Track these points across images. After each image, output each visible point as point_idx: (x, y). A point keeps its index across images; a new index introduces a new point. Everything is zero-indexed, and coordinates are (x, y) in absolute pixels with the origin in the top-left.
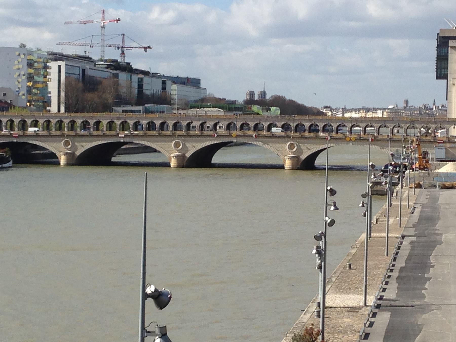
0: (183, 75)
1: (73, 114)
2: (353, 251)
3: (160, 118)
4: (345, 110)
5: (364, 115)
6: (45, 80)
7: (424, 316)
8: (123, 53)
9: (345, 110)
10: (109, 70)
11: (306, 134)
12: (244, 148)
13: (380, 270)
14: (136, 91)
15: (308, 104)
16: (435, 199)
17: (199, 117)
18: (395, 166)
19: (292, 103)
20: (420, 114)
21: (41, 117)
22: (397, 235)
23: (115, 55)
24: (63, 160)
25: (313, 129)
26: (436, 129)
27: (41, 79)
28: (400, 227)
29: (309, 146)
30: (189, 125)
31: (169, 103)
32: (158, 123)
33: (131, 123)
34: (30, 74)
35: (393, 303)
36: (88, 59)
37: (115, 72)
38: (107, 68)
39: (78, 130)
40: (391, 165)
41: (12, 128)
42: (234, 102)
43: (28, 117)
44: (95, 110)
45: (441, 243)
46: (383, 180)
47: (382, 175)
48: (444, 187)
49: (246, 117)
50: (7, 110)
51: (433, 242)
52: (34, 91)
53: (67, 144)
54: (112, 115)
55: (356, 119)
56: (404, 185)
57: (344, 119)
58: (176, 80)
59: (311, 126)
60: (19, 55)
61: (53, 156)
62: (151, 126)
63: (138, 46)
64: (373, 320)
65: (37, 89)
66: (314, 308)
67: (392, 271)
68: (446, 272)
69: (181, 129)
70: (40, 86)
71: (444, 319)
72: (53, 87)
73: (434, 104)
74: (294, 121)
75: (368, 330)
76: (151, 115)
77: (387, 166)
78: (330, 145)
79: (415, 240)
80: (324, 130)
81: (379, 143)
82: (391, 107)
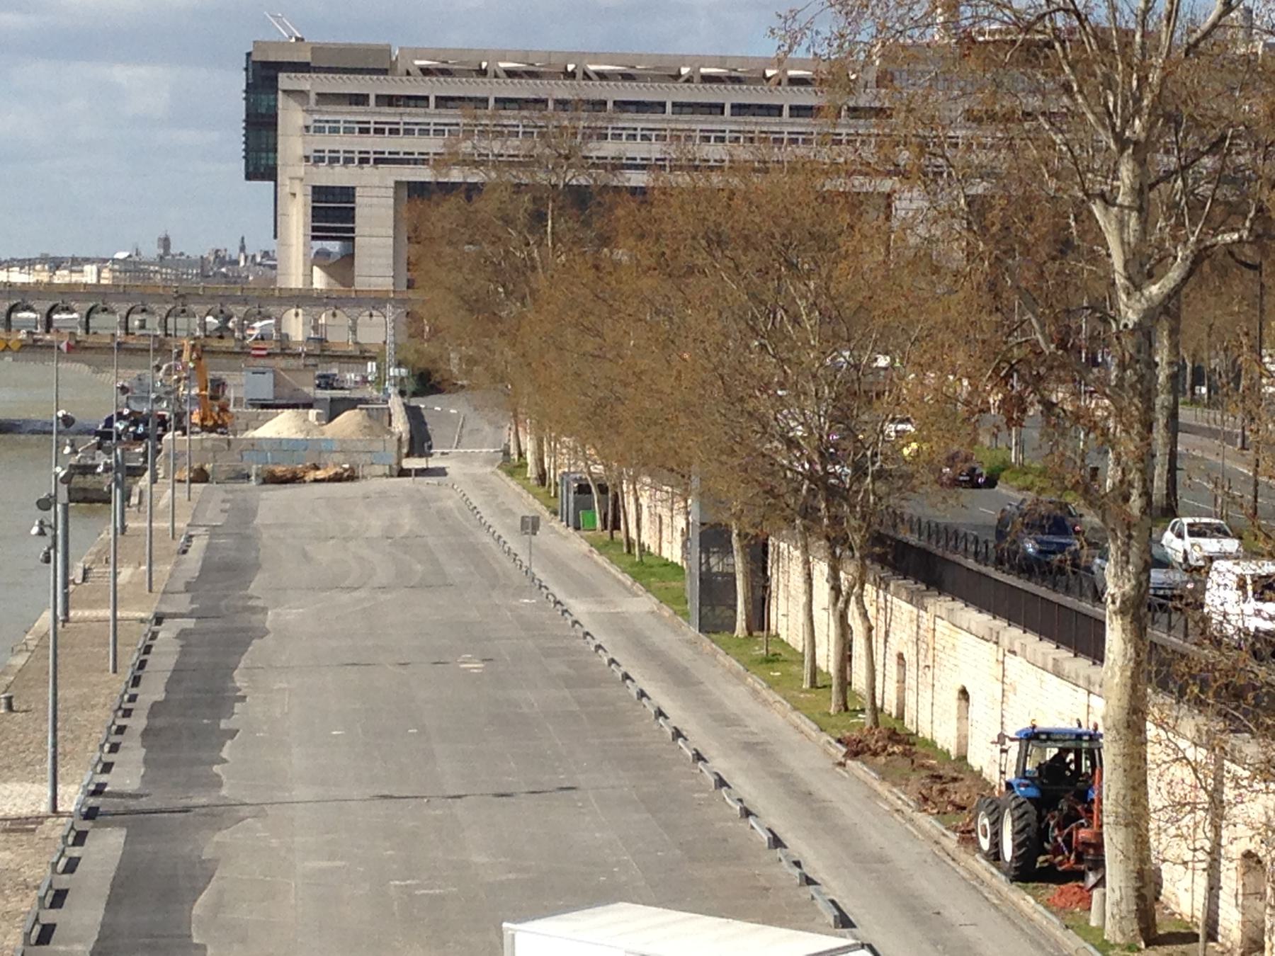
2: (19, 661)
13: (96, 712)
16: (245, 513)
22: (143, 615)
28: (150, 591)
45: (264, 633)
48: (272, 479)
51: (243, 630)
67: (127, 713)
73: (242, 249)
79: (192, 626)
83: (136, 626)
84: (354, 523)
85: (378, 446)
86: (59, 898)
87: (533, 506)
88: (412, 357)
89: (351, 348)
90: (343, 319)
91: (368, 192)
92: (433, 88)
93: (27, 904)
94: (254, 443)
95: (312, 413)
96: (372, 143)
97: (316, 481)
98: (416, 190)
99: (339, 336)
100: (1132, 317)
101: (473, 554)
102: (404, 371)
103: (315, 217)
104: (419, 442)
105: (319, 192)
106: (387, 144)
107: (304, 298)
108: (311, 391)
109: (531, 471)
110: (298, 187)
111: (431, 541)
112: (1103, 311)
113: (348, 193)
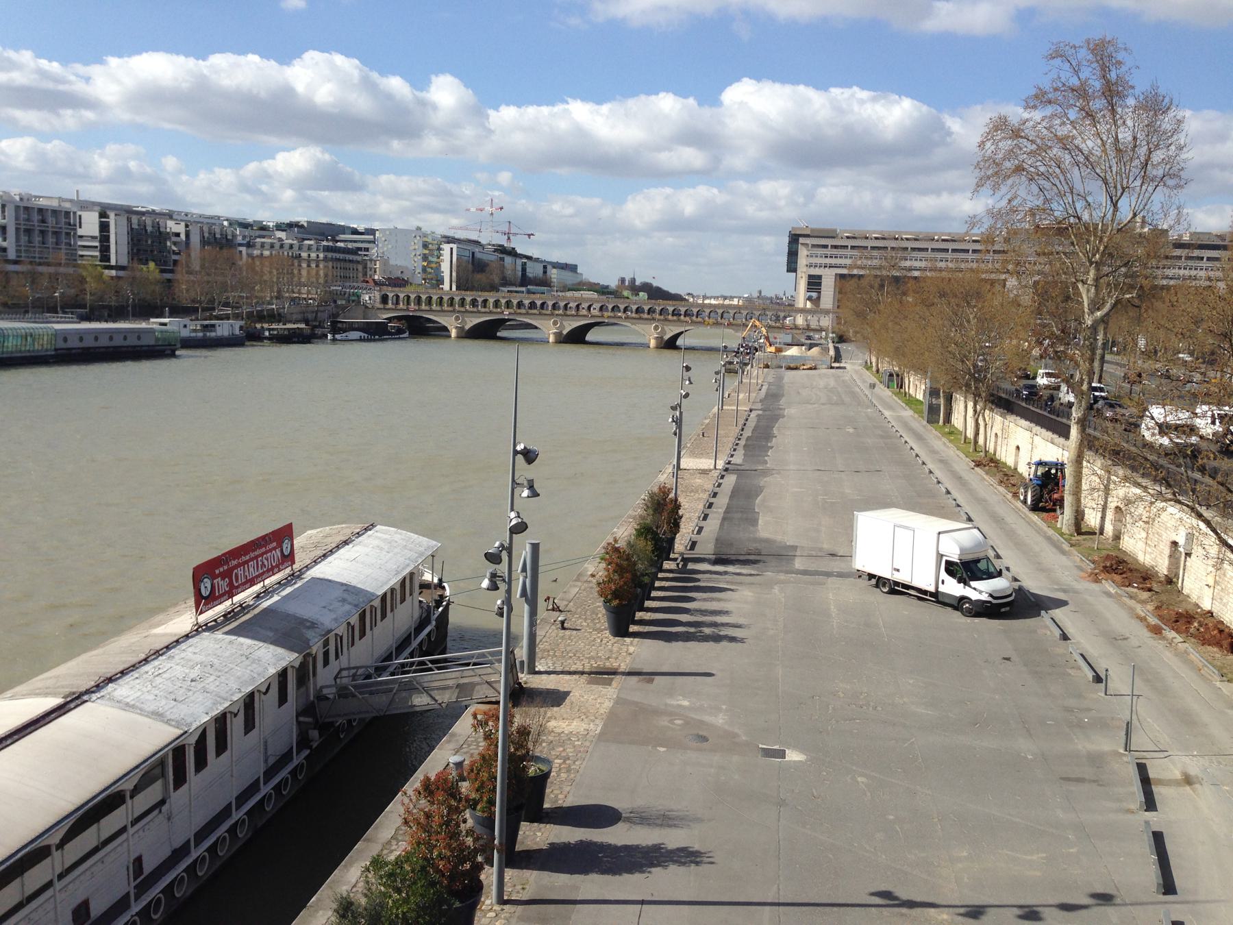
0: (562, 261)
1: (463, 292)
2: (707, 421)
4: (705, 297)
5: (721, 302)
6: (438, 260)
7: (765, 479)
8: (509, 238)
9: (705, 297)
10: (496, 254)
11: (670, 317)
12: (615, 327)
14: (520, 273)
15: (673, 291)
16: (780, 378)
18: (747, 347)
19: (659, 290)
21: (434, 294)
24: (454, 333)
25: (676, 313)
26: (785, 318)
27: (435, 259)
29: (672, 328)
30: (566, 305)
32: (539, 303)
33: (515, 302)
34: (425, 254)
35: (739, 467)
36: (477, 243)
37: (502, 256)
38: (494, 252)
39: (457, 306)
40: (742, 347)
41: (408, 303)
42: (607, 287)
44: (483, 290)
45: (784, 416)
46: (736, 360)
47: (735, 356)
48: (789, 368)
49: (617, 300)
53: (457, 318)
54: (497, 294)
55: (715, 306)
57: (704, 305)
58: (557, 265)
59: (674, 310)
61: (445, 329)
62: (533, 305)
63: (523, 233)
64: (721, 481)
65: (432, 268)
66: (670, 470)
67: (739, 439)
70: (434, 265)
71: (783, 482)
72: (445, 267)
74: (659, 305)
75: (717, 490)
77: (739, 349)
78: (690, 328)
80: (686, 315)
81: (733, 327)
82: (746, 296)
83: (744, 413)
84: (815, 383)
85: (824, 359)
87: (874, 380)
88: (837, 330)
89: (818, 328)
90: (816, 318)
92: (850, 243)
94: (784, 356)
95: (804, 347)
96: (828, 261)
98: (842, 276)
100: (1089, 323)
101: (853, 395)
103: (808, 285)
104: (838, 358)
105: (810, 277)
106: (833, 261)
107: (803, 311)
108: (803, 340)
109: (874, 369)
110: (803, 275)
111: (839, 389)
112: (1079, 320)
113: (820, 277)
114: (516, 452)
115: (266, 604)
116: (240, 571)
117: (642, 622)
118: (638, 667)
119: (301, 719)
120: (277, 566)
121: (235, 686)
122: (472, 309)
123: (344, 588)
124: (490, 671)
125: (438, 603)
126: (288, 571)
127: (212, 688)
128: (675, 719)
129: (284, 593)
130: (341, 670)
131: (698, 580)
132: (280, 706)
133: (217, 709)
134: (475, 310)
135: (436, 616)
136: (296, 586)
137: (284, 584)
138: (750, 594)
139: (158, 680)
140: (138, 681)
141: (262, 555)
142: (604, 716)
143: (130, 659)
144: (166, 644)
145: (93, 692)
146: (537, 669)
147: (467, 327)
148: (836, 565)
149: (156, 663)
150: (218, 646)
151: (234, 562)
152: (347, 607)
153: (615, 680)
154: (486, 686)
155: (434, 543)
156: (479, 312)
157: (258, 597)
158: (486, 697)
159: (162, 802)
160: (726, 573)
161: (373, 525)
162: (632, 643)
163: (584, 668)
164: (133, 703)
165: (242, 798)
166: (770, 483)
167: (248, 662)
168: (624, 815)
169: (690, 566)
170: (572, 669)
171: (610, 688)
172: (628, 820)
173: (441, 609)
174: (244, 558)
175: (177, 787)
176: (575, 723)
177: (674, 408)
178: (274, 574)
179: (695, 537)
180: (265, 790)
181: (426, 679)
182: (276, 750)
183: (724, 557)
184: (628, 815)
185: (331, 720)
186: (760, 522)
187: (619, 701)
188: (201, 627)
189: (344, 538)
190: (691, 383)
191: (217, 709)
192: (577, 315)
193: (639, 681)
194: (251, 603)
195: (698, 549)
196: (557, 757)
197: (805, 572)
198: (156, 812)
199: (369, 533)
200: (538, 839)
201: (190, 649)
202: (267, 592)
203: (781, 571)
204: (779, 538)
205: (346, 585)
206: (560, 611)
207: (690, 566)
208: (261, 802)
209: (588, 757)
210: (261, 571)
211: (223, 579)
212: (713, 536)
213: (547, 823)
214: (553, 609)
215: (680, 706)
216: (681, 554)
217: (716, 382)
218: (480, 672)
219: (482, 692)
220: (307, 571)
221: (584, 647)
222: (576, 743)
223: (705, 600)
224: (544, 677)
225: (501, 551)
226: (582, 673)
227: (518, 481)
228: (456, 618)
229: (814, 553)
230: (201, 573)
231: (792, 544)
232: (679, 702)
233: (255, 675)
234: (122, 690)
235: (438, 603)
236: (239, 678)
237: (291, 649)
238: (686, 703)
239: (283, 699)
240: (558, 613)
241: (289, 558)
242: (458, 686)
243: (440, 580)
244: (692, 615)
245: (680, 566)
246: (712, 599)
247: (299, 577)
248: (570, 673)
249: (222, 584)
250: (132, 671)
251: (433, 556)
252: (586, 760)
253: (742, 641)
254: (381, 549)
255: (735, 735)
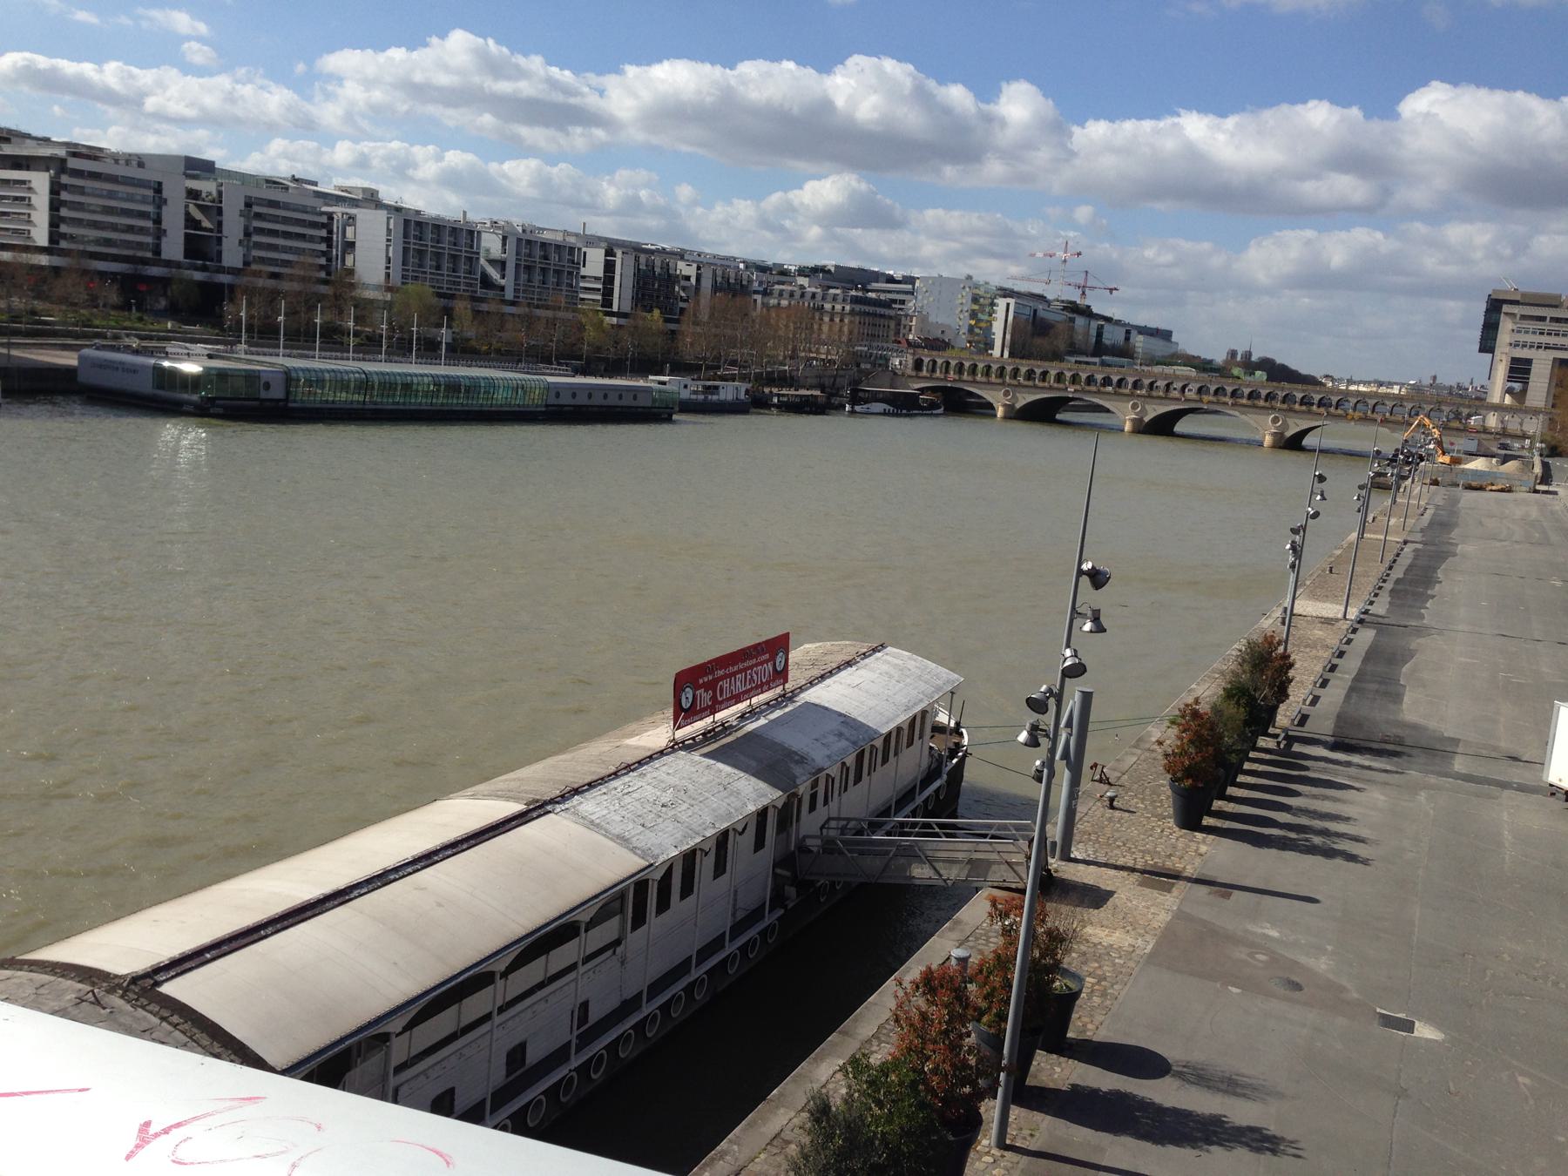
0: (1153, 325)
1: (1018, 361)
2: (1338, 552)
3: (1119, 373)
5: (1374, 389)
6: (989, 319)
7: (1418, 641)
8: (1084, 293)
9: (1350, 382)
11: (1297, 407)
14: (1094, 339)
15: (1304, 371)
16: (1454, 501)
17: (1166, 377)
18: (1410, 454)
20: (1451, 394)
21: (981, 361)
23: (1075, 296)
24: (1000, 412)
25: (1306, 401)
26: (1469, 416)
27: (985, 317)
30: (1152, 384)
31: (1132, 358)
32: (1115, 379)
33: (1084, 376)
34: (973, 311)
35: (1380, 620)
36: (1041, 298)
37: (1071, 315)
38: (1063, 310)
41: (947, 371)
42: (1210, 362)
43: (967, 359)
44: (1043, 358)
45: (1455, 555)
46: (1389, 471)
48: (1469, 487)
49: (1223, 380)
50: (944, 349)
51: (1443, 552)
52: (977, 330)
53: (1007, 393)
54: (1063, 365)
56: (1416, 479)
57: (1348, 393)
58: (1143, 331)
59: (1303, 398)
60: (964, 288)
61: (990, 406)
62: (1107, 381)
63: (1102, 286)
64: (1352, 636)
65: (981, 328)
66: (1278, 613)
67: (1384, 581)
68: (1456, 591)
69: (1141, 388)
70: (983, 325)
72: (998, 328)
73: (1471, 383)
74: (1283, 389)
75: (1345, 648)
76: (1108, 369)
77: (1396, 455)
80: (1320, 404)
81: (1390, 425)
82: (1412, 382)
83: (1394, 544)
84: (1507, 511)
85: (1525, 478)
86: (1341, 654)
88: (1549, 438)
89: (1519, 433)
90: (1517, 419)
91: (1539, 361)
93: (1327, 654)
94: (1463, 470)
95: (1494, 460)
96: (1545, 339)
97: (1491, 490)
99: (1513, 425)
102: (1544, 445)
103: (1510, 372)
104: (1546, 478)
105: (1514, 360)
106: (1552, 340)
108: (1495, 450)
110: (1504, 358)
111: (1545, 524)
113: (1529, 362)
114: (1080, 572)
115: (751, 727)
116: (725, 684)
117: (1220, 815)
118: (1210, 873)
119: (779, 871)
120: (768, 683)
121: (709, 820)
122: (1027, 383)
123: (842, 719)
124: (1011, 848)
125: (953, 753)
126: (779, 690)
127: (684, 817)
128: (1257, 953)
129: (773, 716)
130: (829, 819)
131: (1307, 769)
132: (756, 851)
133: (688, 844)
134: (1030, 383)
135: (948, 768)
136: (787, 710)
137: (773, 706)
138: (1382, 798)
139: (627, 799)
140: (605, 797)
141: (751, 668)
142: (1158, 932)
143: (599, 770)
144: (639, 759)
145: (558, 803)
146: (1072, 856)
147: (1018, 406)
148: (1516, 774)
149: (626, 779)
150: (694, 769)
151: (721, 673)
152: (844, 743)
153: (1177, 886)
154: (1005, 867)
155: (956, 676)
156: (1035, 387)
157: (742, 717)
158: (1004, 881)
159: (617, 943)
160: (1348, 764)
161: (883, 646)
162: (1204, 842)
163: (1135, 864)
164: (598, 821)
165: (705, 953)
166: (1427, 650)
167: (725, 794)
168: (1175, 1068)
169: (1297, 748)
170: (1119, 863)
171: (1169, 895)
172: (1180, 1075)
173: (955, 761)
174: (732, 669)
175: (634, 928)
176: (1117, 934)
177: (1295, 531)
178: (762, 692)
179: (1306, 709)
180: (730, 948)
181: (930, 846)
182: (748, 901)
183: (1347, 741)
184: (1180, 1069)
185: (812, 878)
186: (1406, 699)
187: (1180, 915)
188: (677, 744)
189: (848, 658)
190: (1323, 498)
191: (688, 844)
192: (1166, 398)
193: (1210, 893)
194: (734, 724)
195: (1309, 726)
196: (1089, 975)
197: (1468, 778)
198: (610, 953)
199: (878, 655)
200: (1056, 1076)
201: (664, 768)
202: (753, 713)
203: (1432, 772)
204: (1432, 724)
205: (845, 716)
206: (1109, 784)
207: (1297, 748)
208: (724, 961)
209: (1131, 981)
210: (749, 687)
211: (706, 691)
212: (1335, 710)
213: (1069, 1058)
214: (1101, 781)
215: (1266, 936)
216: (1285, 730)
217: (1358, 499)
218: (1000, 847)
219: (999, 874)
220: (800, 693)
221: (1138, 835)
222: (1117, 961)
223: (1315, 797)
224: (1081, 867)
225: (1048, 698)
226: (1133, 870)
227: (1079, 610)
228: (974, 775)
229: (1484, 752)
230: (685, 679)
231: (1452, 736)
232: (1266, 931)
233: (732, 810)
234: (588, 804)
235: (953, 754)
236: (714, 810)
237: (775, 785)
238: (1274, 933)
239: (759, 843)
240: (1107, 787)
241: (782, 675)
242: (970, 861)
243: (958, 724)
244: (1294, 815)
245: (1282, 746)
246: (1325, 798)
247: (791, 699)
248: (1116, 867)
249: (705, 697)
250: (601, 784)
251: (952, 693)
252: (1128, 985)
253: (1365, 862)
254: (891, 677)
255: (1343, 989)
